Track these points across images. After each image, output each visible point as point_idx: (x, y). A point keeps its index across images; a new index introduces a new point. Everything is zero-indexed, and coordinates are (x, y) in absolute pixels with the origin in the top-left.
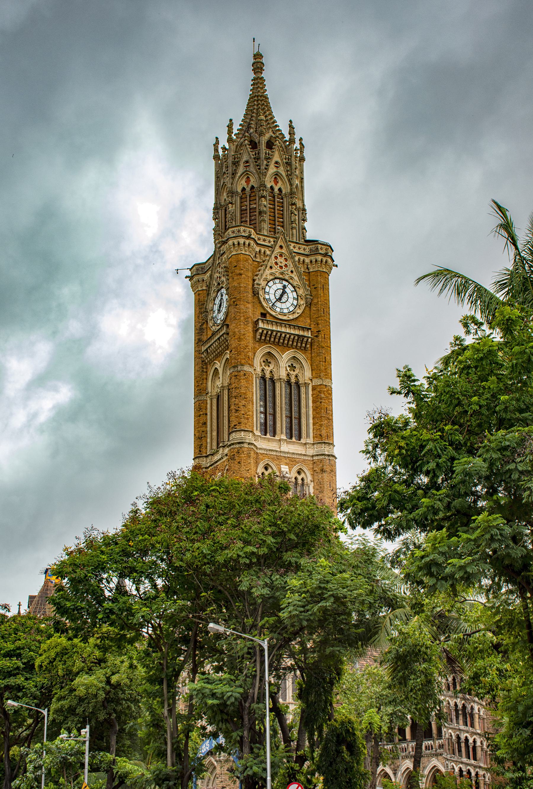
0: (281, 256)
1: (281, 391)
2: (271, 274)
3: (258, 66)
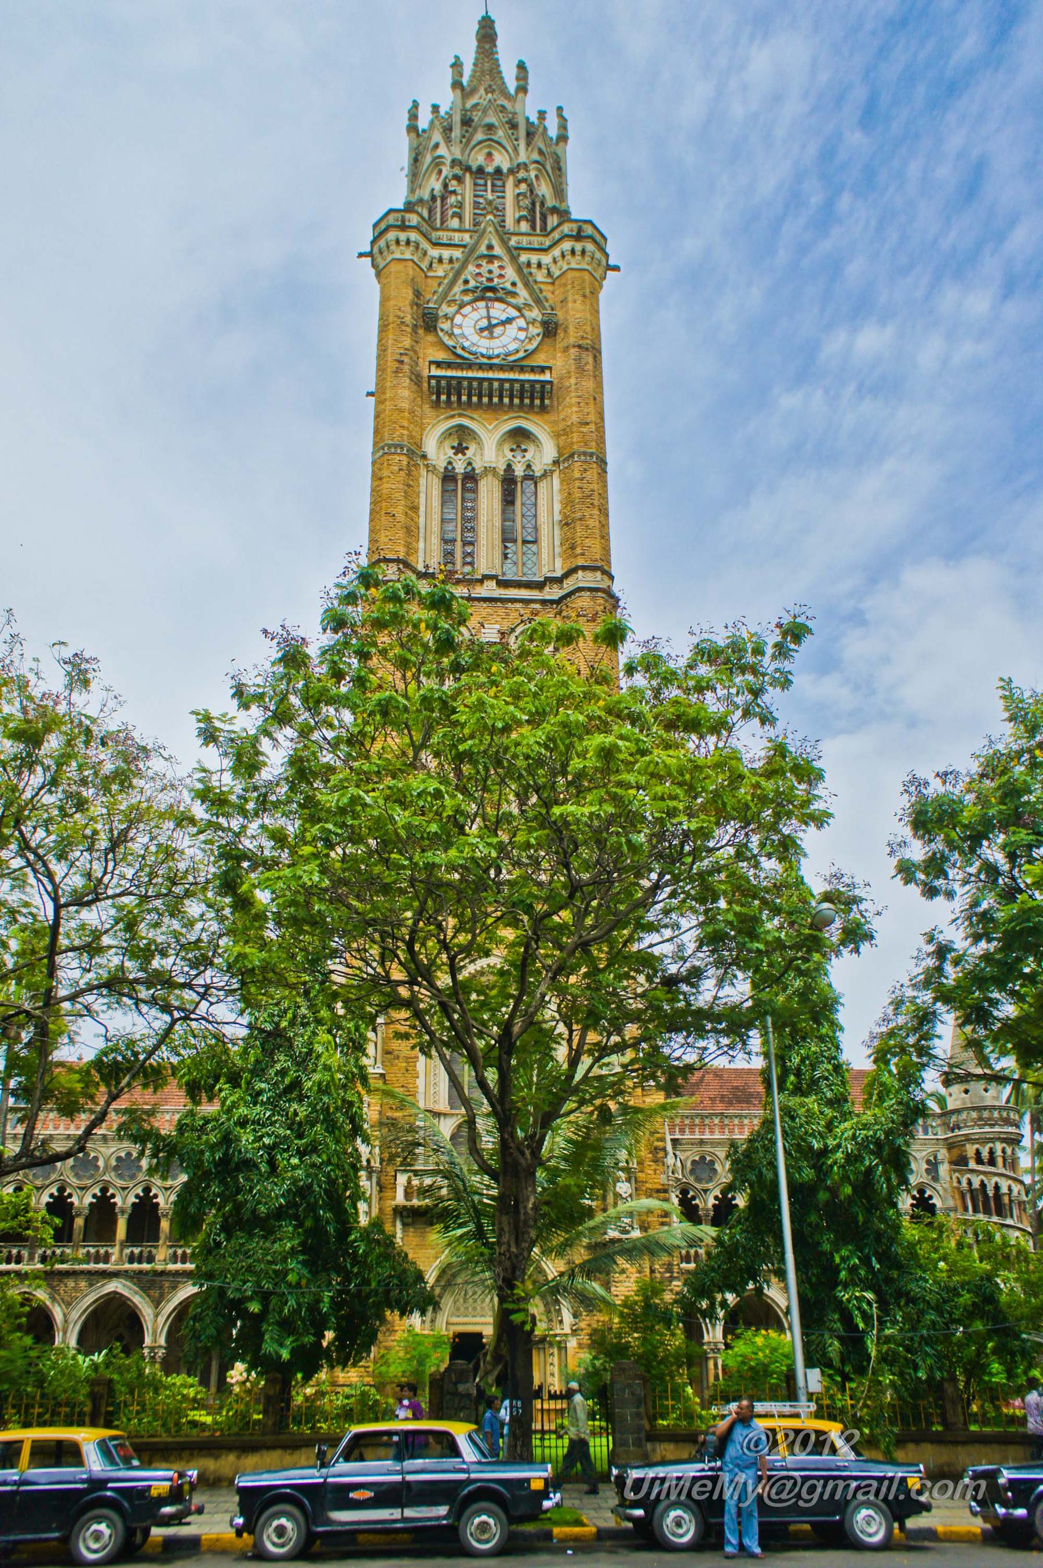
1: (489, 493)
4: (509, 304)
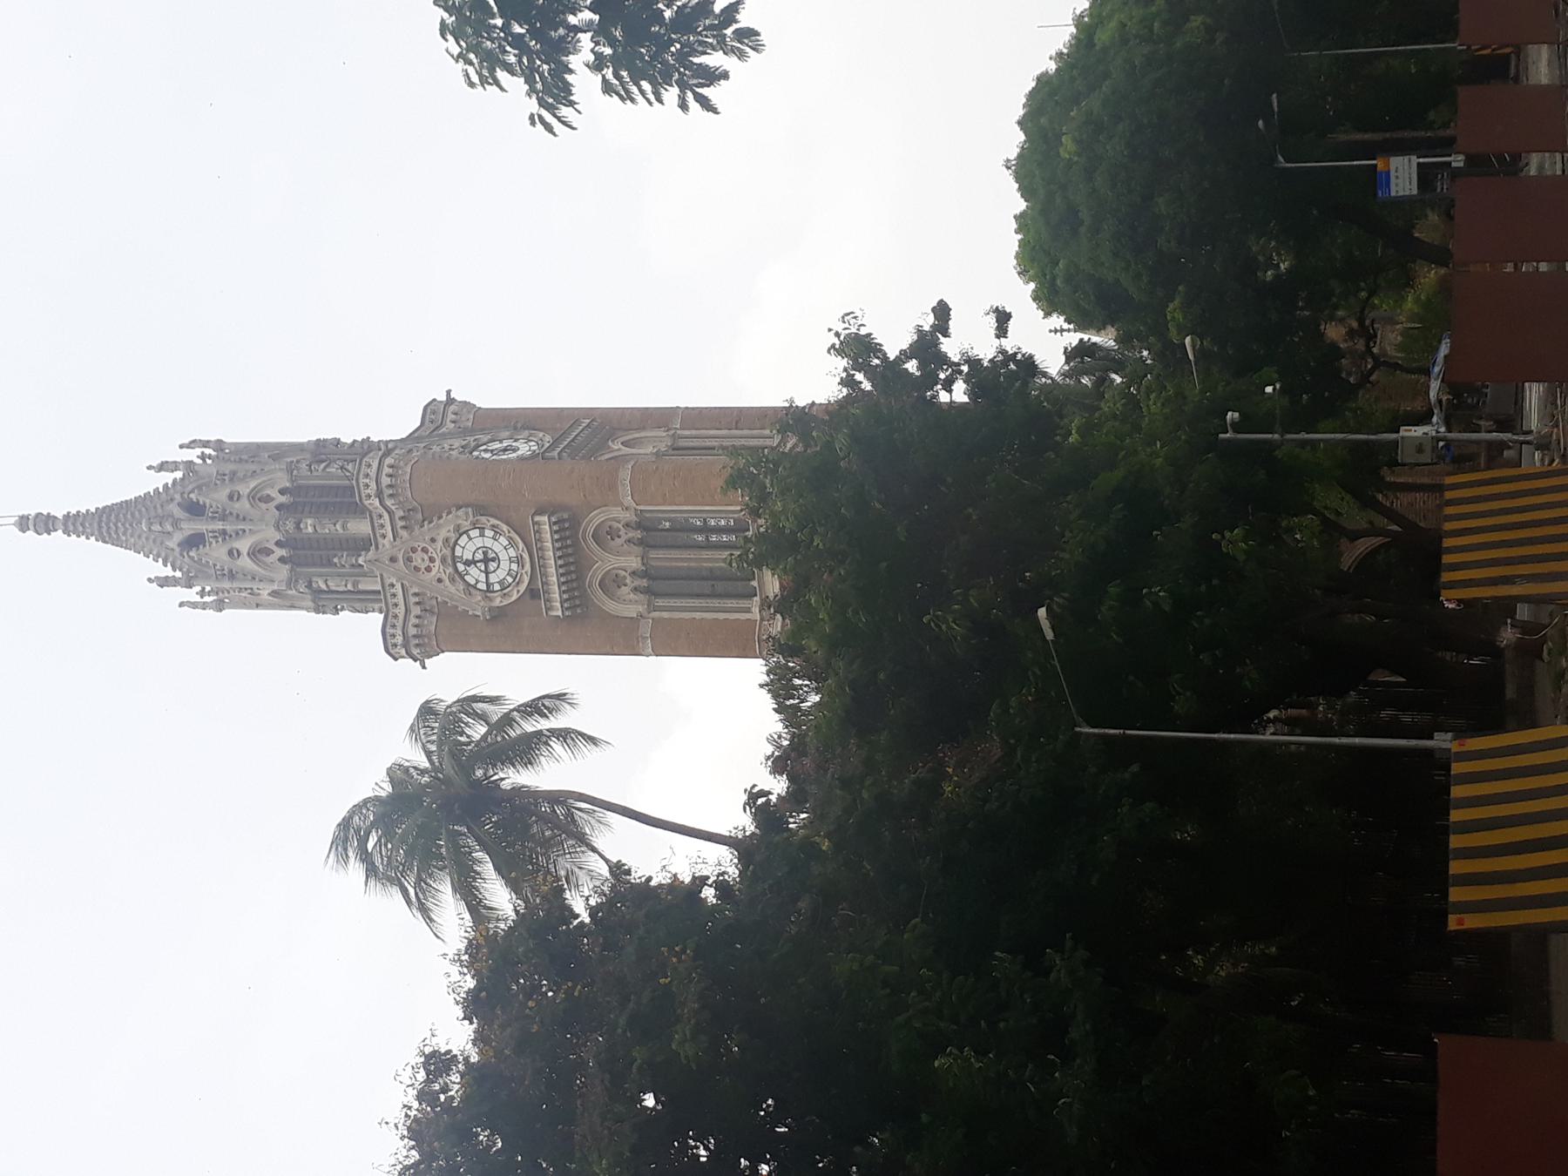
0: (410, 560)
1: (662, 558)
2: (452, 580)
3: (43, 524)
4: (456, 543)
